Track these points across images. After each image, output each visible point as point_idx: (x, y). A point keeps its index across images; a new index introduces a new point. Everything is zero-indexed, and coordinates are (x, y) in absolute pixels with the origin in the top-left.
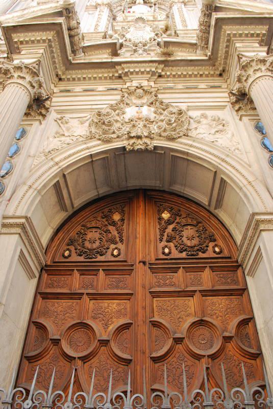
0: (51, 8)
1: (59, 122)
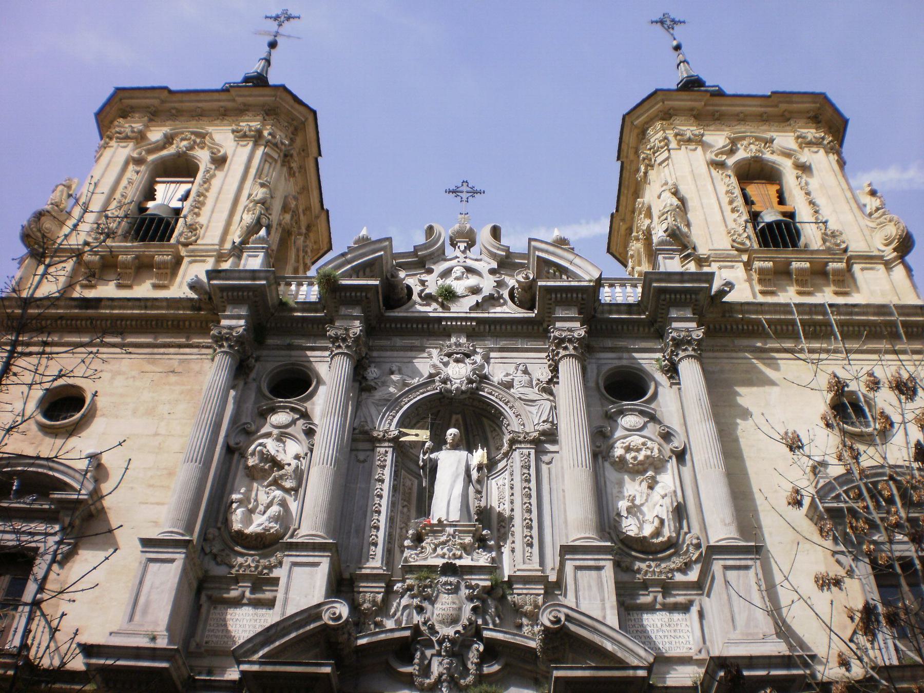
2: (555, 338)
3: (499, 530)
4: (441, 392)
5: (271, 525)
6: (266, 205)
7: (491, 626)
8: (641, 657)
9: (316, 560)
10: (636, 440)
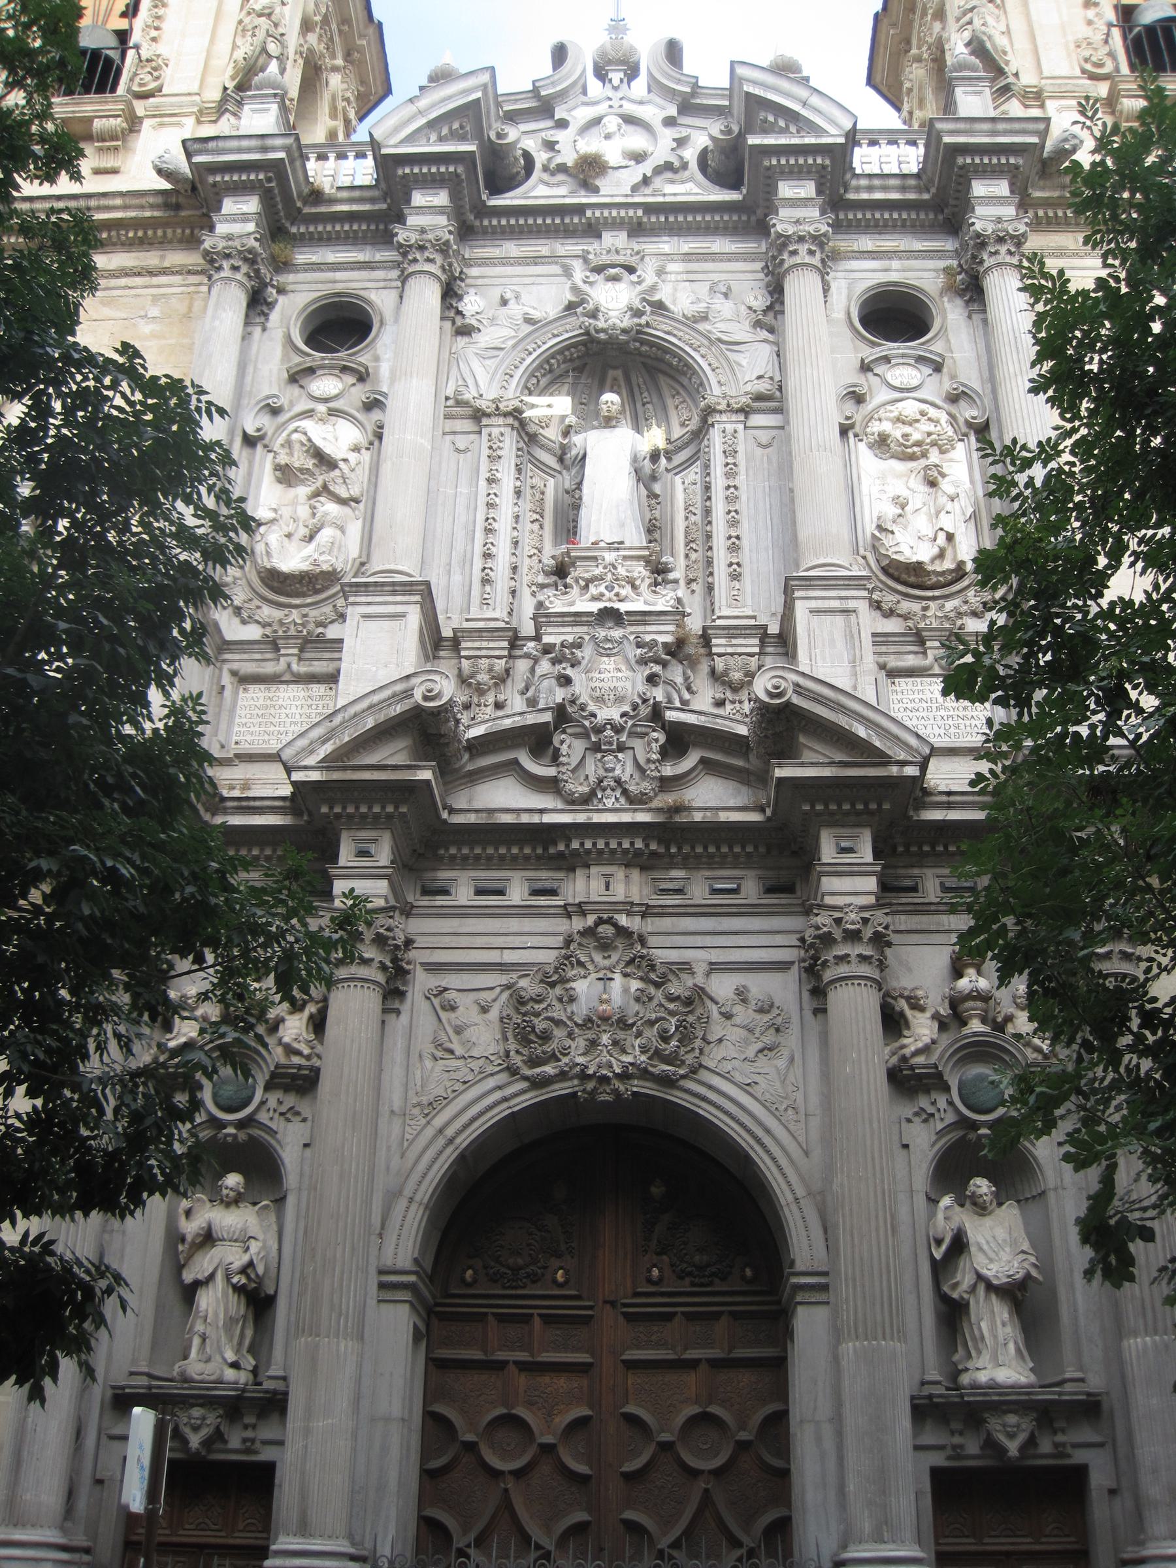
0: (394, 695)
1: (436, 1001)
2: (779, 236)
3: (687, 556)
4: (587, 333)
5: (322, 558)
6: (273, 18)
7: (678, 704)
8: (911, 747)
9: (399, 609)
10: (910, 408)
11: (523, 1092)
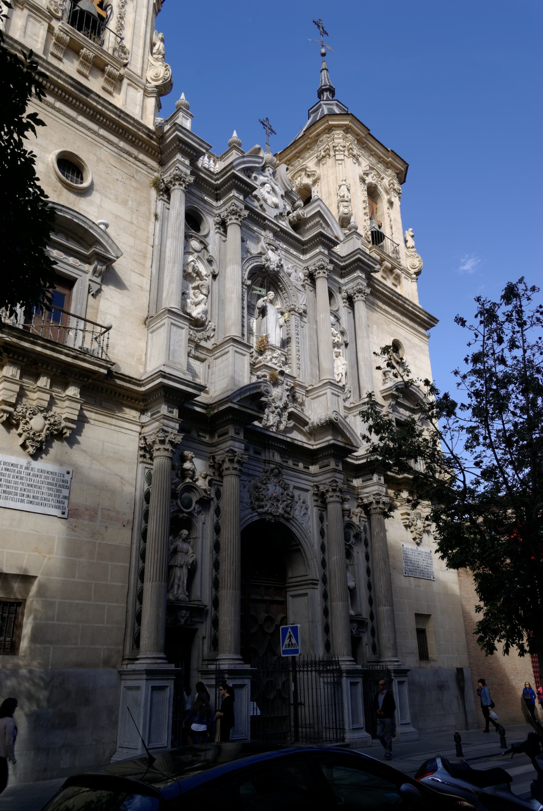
11: (256, 516)
